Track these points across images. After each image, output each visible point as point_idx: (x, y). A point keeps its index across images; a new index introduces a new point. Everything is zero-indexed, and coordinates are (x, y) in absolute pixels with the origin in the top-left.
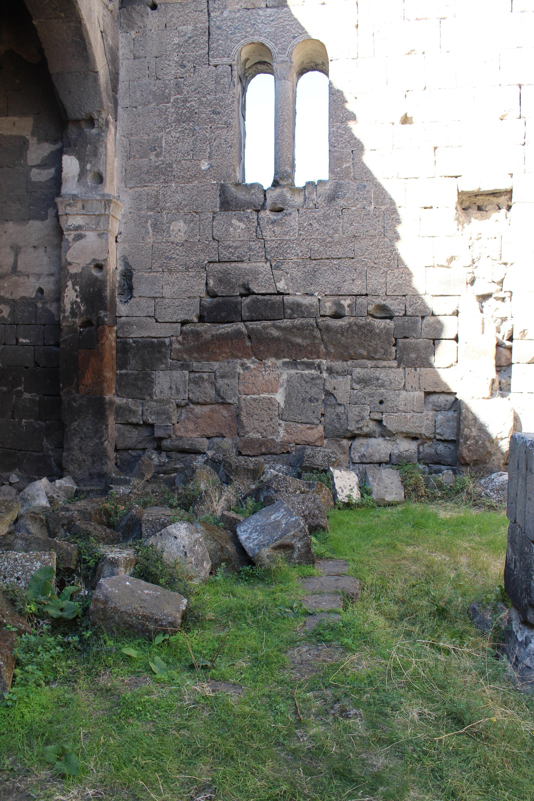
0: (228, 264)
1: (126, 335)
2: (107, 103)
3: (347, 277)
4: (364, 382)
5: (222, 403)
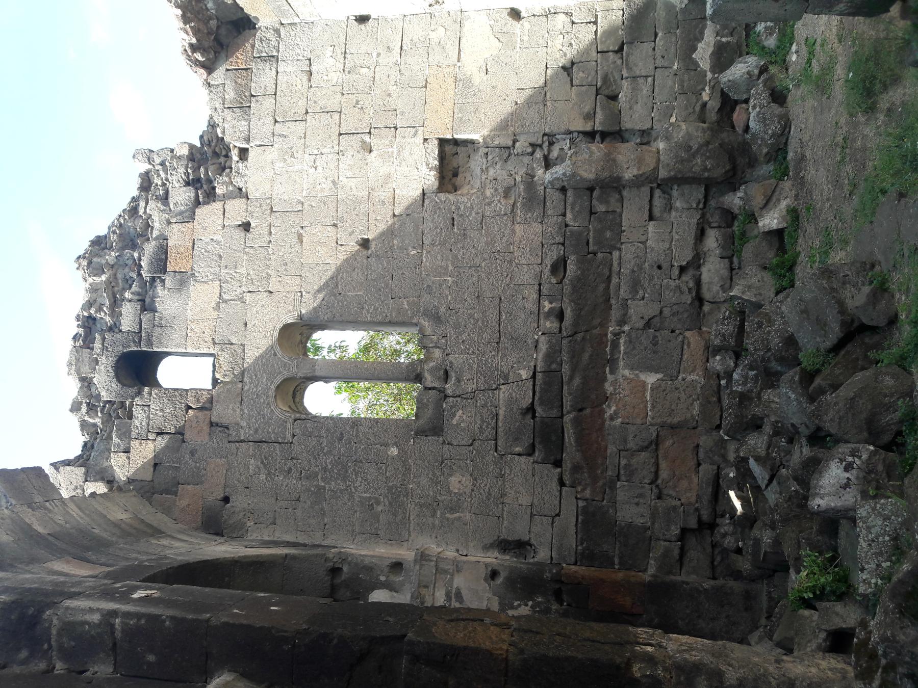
0: (500, 430)
1: (573, 553)
3: (521, 304)
4: (635, 285)
5: (657, 445)
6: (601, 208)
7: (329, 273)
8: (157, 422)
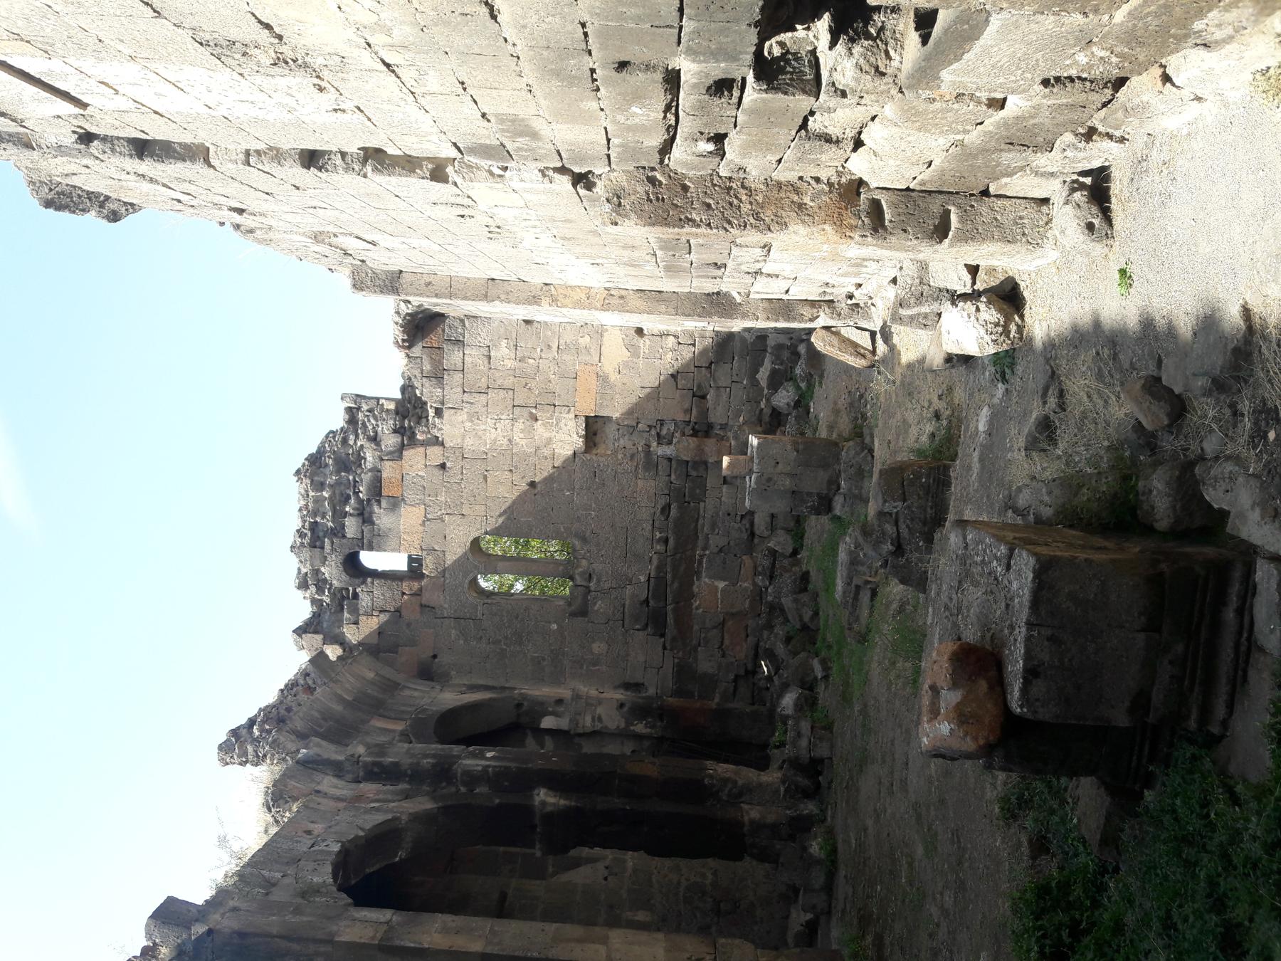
2: (507, 694)
4: (714, 526)
6: (694, 473)
7: (507, 504)
8: (380, 603)
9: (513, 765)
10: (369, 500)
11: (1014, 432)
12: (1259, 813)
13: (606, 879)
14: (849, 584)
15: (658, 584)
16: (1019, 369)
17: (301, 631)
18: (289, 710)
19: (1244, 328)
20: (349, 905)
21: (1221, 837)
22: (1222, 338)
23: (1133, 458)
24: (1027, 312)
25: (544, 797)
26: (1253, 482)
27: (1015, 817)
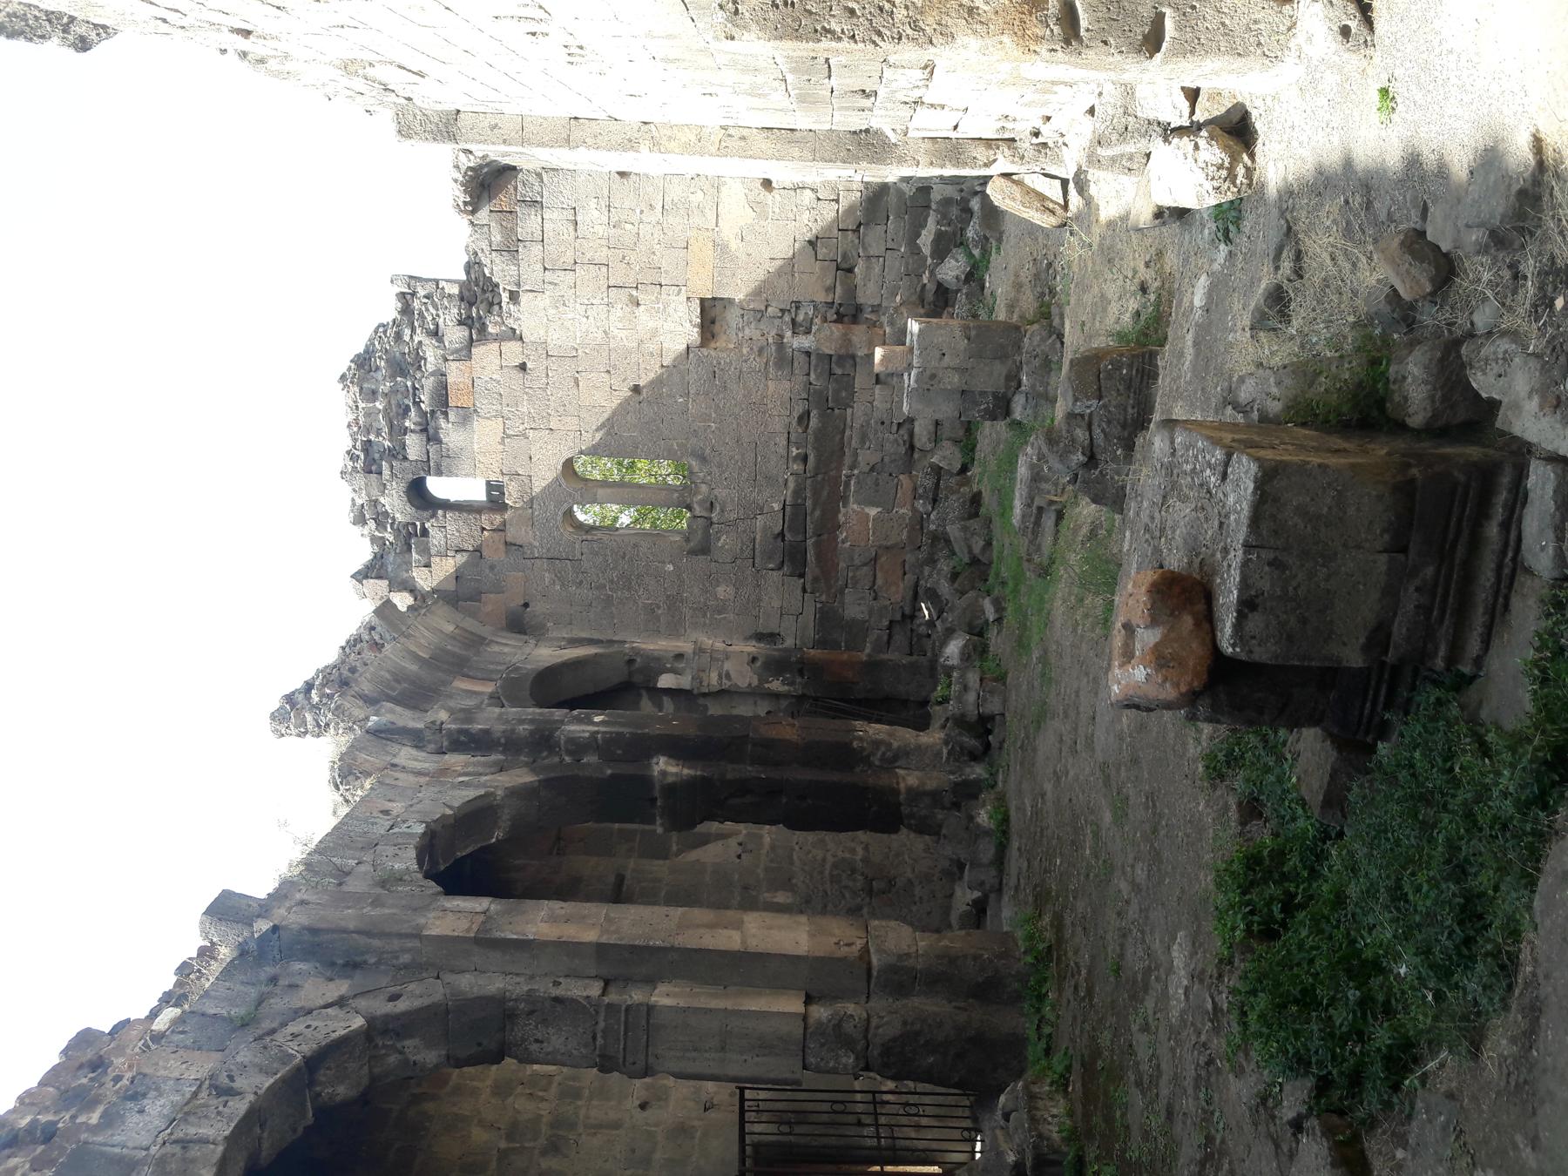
2: (615, 648)
4: (864, 438)
7: (606, 416)
8: (455, 541)
9: (625, 730)
10: (433, 412)
11: (1237, 306)
12: (1513, 766)
13: (739, 857)
14: (1029, 506)
15: (795, 514)
16: (1247, 225)
17: (362, 575)
18: (353, 670)
19: (1533, 162)
20: (439, 893)
21: (1465, 794)
22: (1506, 177)
23: (1385, 337)
24: (1259, 149)
25: (664, 767)
26: (1534, 364)
27: (1222, 777)
